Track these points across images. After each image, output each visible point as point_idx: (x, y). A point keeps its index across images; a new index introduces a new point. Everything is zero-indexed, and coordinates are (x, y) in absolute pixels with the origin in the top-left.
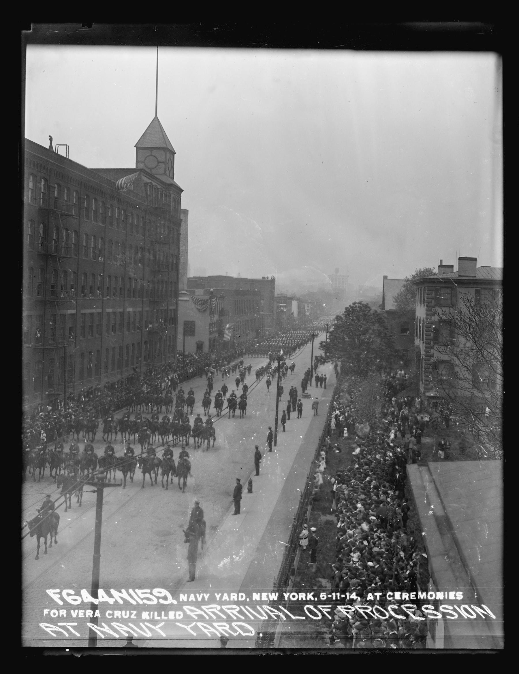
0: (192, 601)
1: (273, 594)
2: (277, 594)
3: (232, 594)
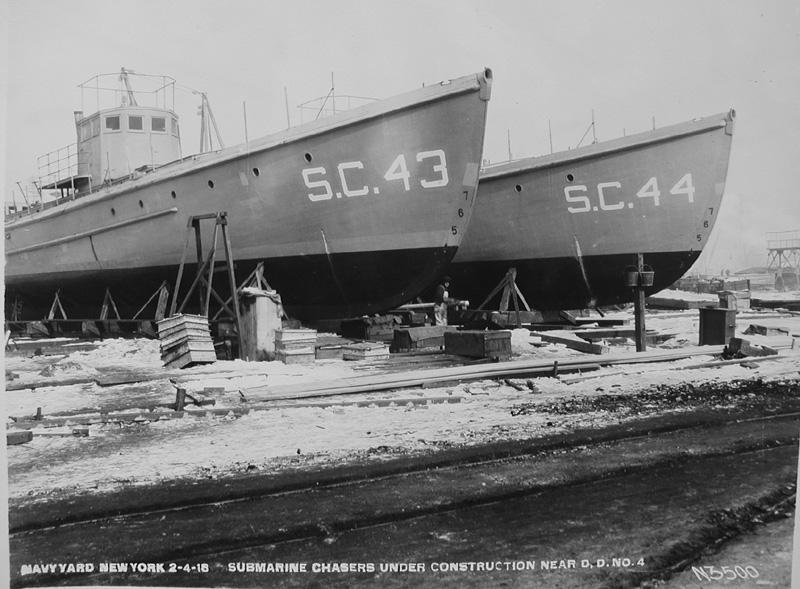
1: (122, 564)
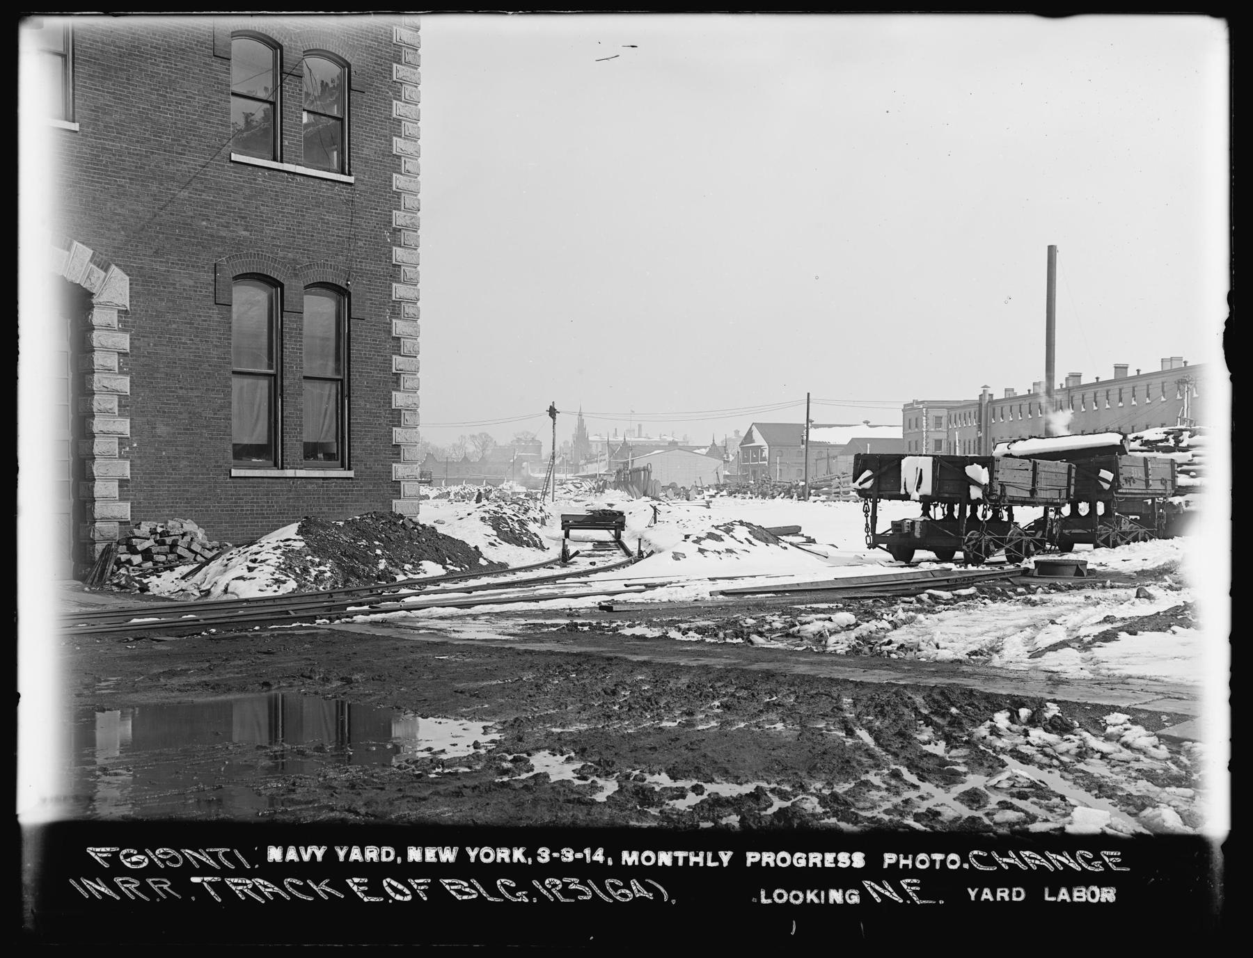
0: (292, 861)
2: (456, 849)
3: (368, 849)
